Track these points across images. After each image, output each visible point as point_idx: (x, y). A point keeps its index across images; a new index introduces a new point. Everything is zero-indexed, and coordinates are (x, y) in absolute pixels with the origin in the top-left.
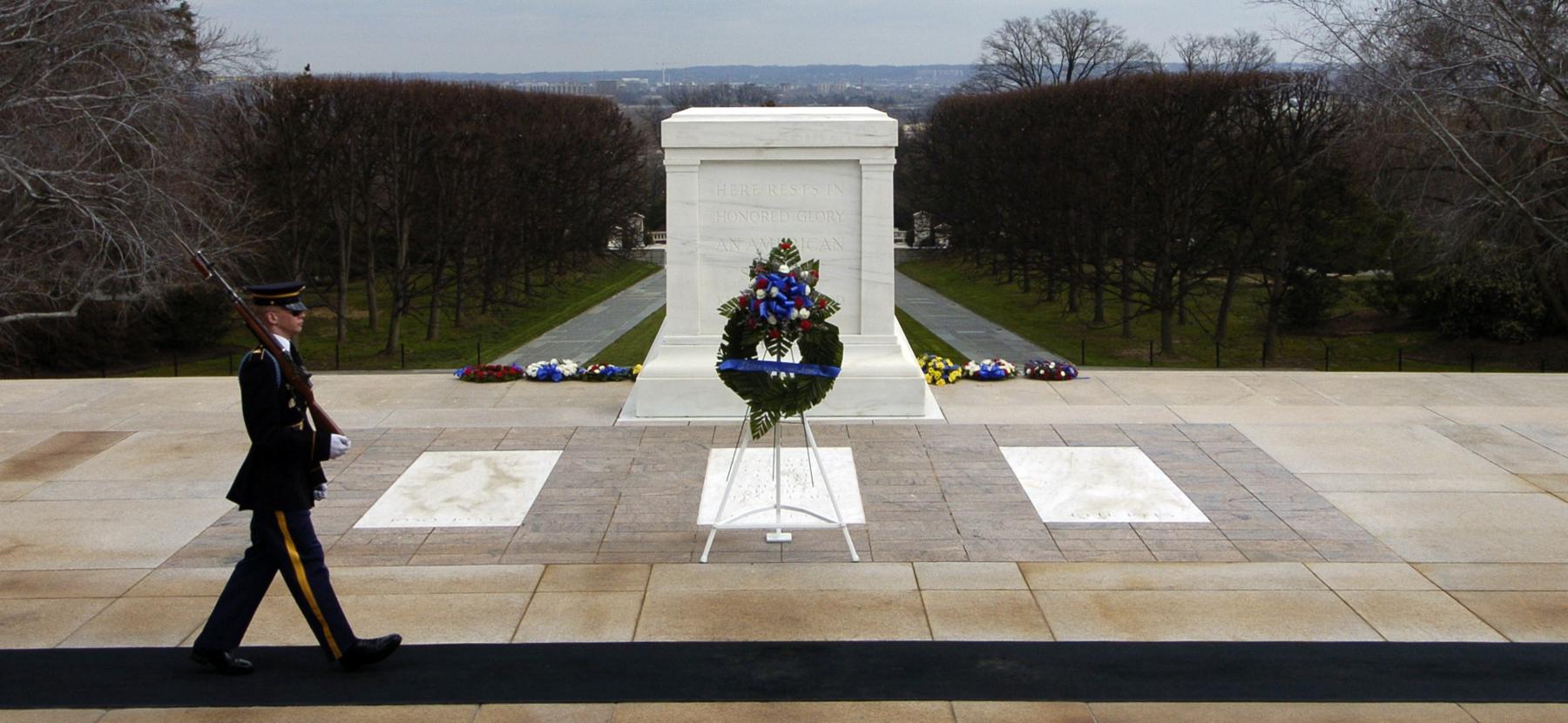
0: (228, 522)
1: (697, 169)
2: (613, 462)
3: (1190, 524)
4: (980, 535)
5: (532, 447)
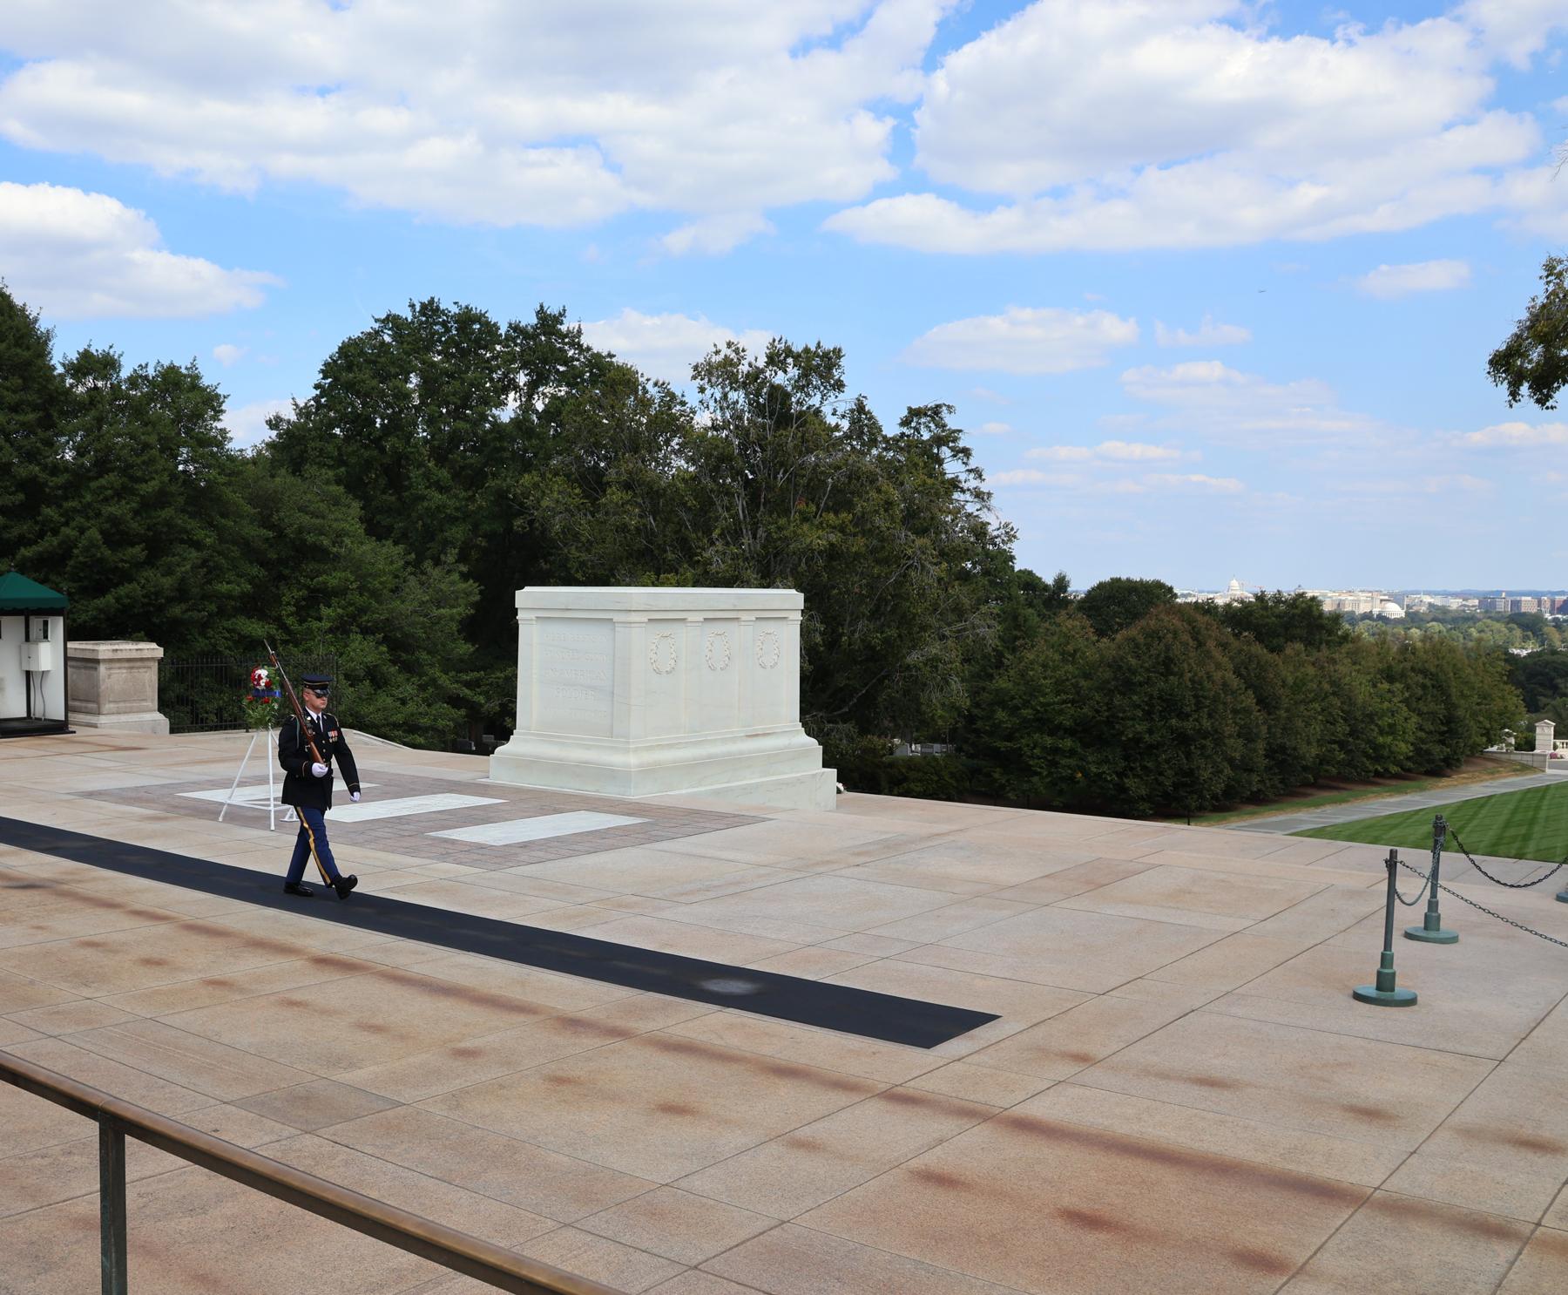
1: (534, 622)
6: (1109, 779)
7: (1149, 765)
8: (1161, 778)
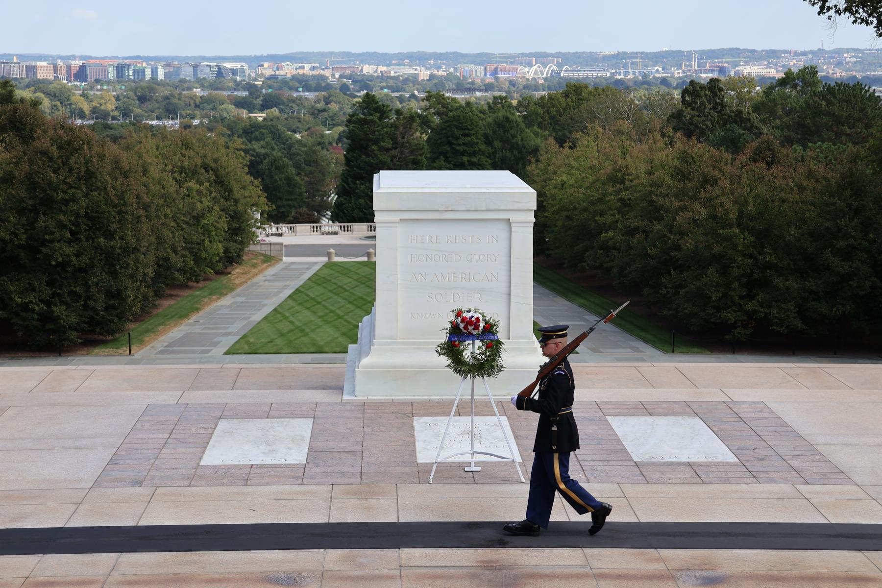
0: (117, 462)
2: (349, 426)
3: (727, 463)
4: (595, 468)
5: (293, 416)
6: (37, 308)
7: (78, 289)
8: (91, 303)
